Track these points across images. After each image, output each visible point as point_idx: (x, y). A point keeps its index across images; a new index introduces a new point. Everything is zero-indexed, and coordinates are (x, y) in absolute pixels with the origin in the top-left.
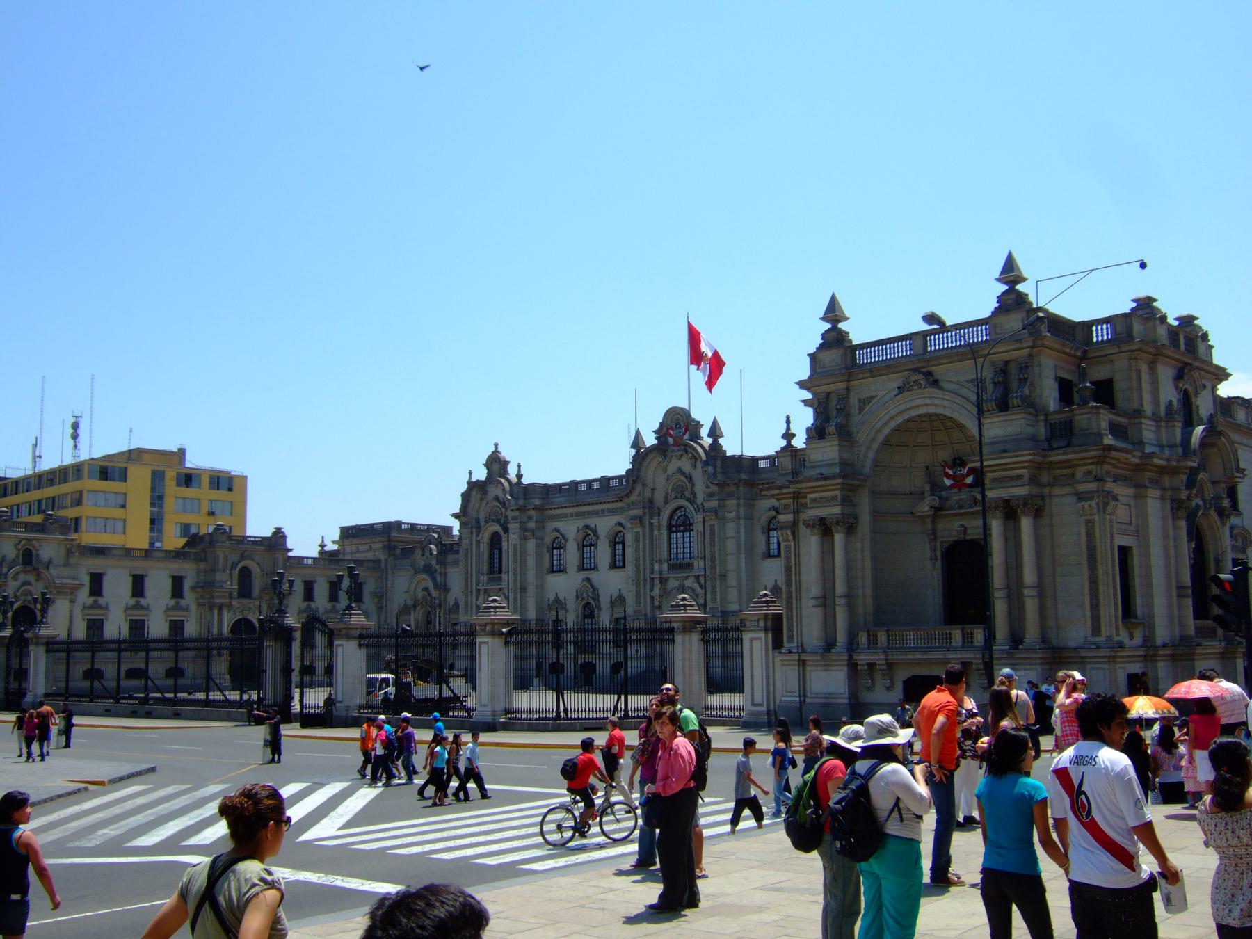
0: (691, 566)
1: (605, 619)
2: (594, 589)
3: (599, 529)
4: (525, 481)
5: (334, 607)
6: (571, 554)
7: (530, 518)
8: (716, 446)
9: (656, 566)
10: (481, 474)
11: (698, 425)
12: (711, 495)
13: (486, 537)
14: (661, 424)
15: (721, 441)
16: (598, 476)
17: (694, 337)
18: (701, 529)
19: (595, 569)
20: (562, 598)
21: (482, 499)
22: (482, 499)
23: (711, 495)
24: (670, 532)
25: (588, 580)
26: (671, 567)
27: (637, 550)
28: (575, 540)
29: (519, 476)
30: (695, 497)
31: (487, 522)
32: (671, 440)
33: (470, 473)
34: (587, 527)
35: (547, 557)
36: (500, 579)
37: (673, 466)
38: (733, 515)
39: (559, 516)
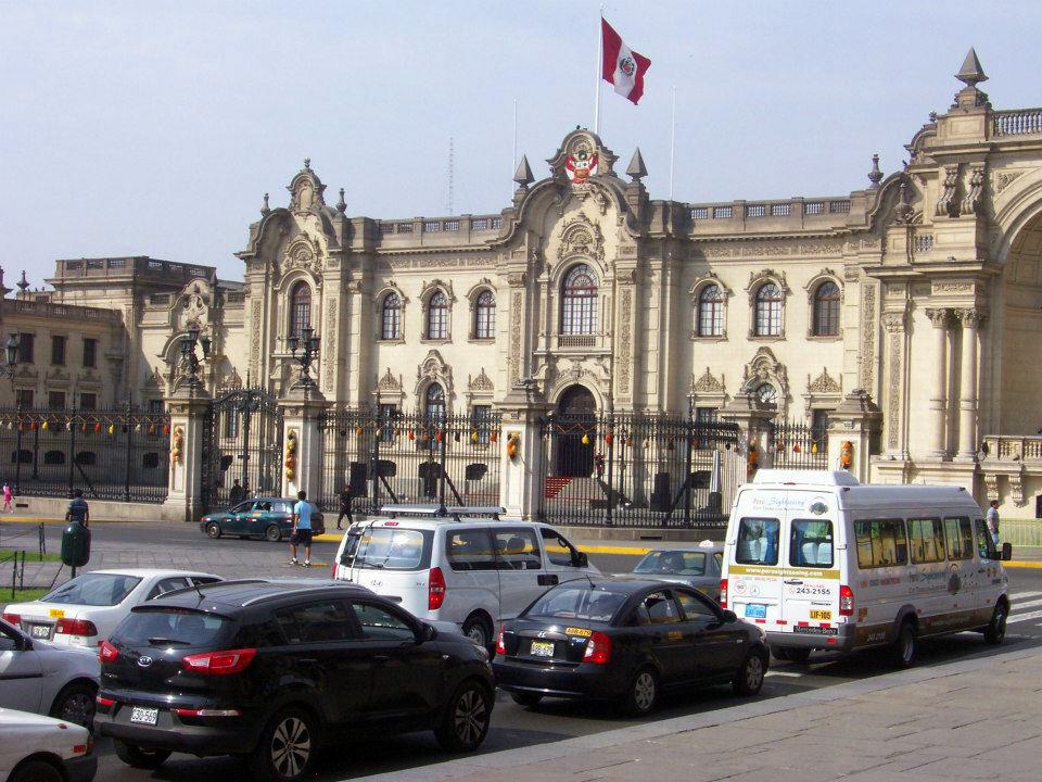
0: (591, 341)
1: (460, 407)
2: (445, 369)
4: (349, 213)
5: (58, 371)
6: (412, 318)
7: (354, 266)
9: (542, 342)
10: (281, 200)
11: (612, 159)
12: (627, 251)
14: (559, 151)
15: (644, 180)
17: (611, 41)
18: (610, 294)
19: (449, 340)
20: (396, 376)
21: (282, 236)
24: (563, 296)
27: (517, 311)
29: (343, 207)
30: (602, 252)
32: (571, 175)
33: (266, 198)
34: (439, 282)
35: (377, 318)
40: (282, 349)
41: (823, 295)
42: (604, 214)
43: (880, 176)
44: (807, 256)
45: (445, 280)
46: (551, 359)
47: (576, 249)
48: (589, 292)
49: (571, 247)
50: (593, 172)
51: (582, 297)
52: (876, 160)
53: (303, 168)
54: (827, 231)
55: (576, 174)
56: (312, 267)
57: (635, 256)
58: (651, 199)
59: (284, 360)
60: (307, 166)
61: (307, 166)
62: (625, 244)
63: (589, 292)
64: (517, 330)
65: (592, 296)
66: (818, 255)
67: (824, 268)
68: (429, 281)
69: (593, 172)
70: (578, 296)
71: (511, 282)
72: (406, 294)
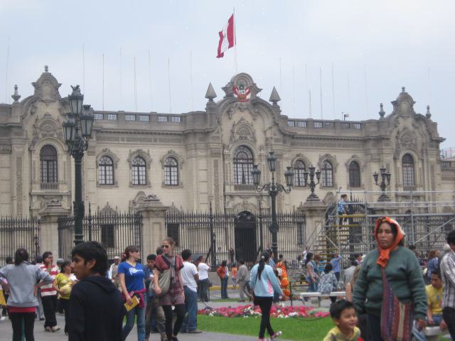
3: (151, 153)
8: (278, 109)
9: (227, 187)
12: (277, 140)
13: (38, 149)
15: (279, 103)
16: (148, 111)
22: (32, 113)
23: (277, 140)
25: (143, 193)
26: (237, 187)
27: (216, 172)
28: (129, 161)
30: (255, 141)
31: (35, 134)
32: (236, 96)
36: (56, 187)
37: (237, 116)
39: (109, 139)
40: (37, 190)
45: (145, 150)
46: (232, 196)
47: (241, 138)
49: (237, 137)
50: (248, 97)
51: (242, 164)
53: (44, 72)
55: (239, 97)
56: (56, 136)
57: (281, 143)
59: (40, 196)
60: (47, 71)
61: (47, 71)
62: (276, 137)
64: (216, 180)
68: (134, 150)
69: (248, 97)
70: (240, 163)
71: (212, 153)
72: (119, 157)
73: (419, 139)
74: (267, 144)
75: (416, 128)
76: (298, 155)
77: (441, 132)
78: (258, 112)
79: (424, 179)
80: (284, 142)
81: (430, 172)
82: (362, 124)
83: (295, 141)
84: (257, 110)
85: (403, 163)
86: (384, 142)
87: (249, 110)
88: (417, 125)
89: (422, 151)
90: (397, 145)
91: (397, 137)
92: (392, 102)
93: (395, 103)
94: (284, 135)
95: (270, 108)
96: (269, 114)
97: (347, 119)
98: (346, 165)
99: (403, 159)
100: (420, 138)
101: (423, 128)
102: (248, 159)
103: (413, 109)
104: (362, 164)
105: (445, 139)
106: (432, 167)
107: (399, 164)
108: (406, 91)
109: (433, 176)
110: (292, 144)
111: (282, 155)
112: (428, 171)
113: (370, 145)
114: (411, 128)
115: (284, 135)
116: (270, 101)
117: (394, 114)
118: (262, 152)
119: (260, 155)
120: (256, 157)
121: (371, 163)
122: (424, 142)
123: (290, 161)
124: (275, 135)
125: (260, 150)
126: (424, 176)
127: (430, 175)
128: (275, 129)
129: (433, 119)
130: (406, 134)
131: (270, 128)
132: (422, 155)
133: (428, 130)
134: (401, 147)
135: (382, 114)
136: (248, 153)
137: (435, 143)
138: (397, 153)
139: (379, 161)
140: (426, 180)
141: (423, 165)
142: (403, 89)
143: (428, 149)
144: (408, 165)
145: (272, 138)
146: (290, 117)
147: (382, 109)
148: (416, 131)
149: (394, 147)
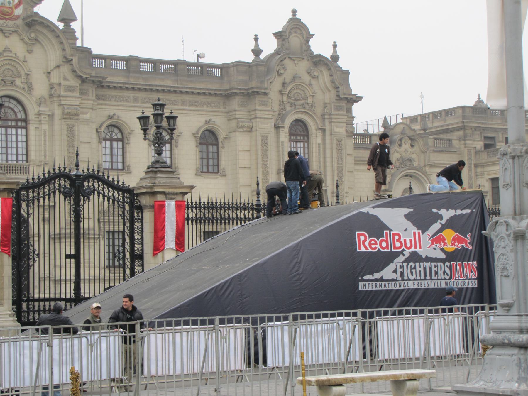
8: (70, 33)
12: (70, 89)
18: (45, 127)
30: (30, 88)
38: (88, 116)
41: (209, 139)
42: (30, 51)
43: (261, 51)
44: (191, 108)
48: (14, 124)
50: (19, 11)
52: (256, 39)
54: (215, 90)
57: (78, 94)
58: (78, 43)
63: (14, 124)
65: (16, 127)
66: (202, 109)
67: (208, 119)
69: (19, 11)
73: (319, 96)
74: (51, 96)
75: (313, 78)
76: (110, 117)
77: (356, 86)
78: (36, 40)
79: (325, 162)
80: (83, 92)
81: (335, 151)
82: (224, 68)
83: (102, 92)
84: (33, 35)
85: (290, 135)
86: (259, 99)
87: (20, 35)
88: (316, 74)
89: (323, 115)
90: (282, 104)
91: (281, 92)
92: (275, 34)
93: (278, 35)
94: (84, 81)
95: (63, 34)
96: (54, 41)
97: (201, 61)
98: (195, 135)
99: (290, 129)
100: (321, 92)
101: (325, 77)
102: (17, 121)
103: (309, 46)
104: (221, 136)
105: (361, 98)
106: (339, 142)
107: (284, 136)
108: (298, 16)
109: (340, 157)
110: (99, 98)
111: (77, 115)
112: (332, 148)
113: (235, 103)
114: (307, 78)
115: (84, 81)
116: (61, 20)
117: (277, 53)
118: (42, 109)
119: (39, 114)
120: (32, 116)
121: (237, 133)
122: (327, 101)
123: (94, 126)
124: (65, 79)
125: (40, 105)
126: (325, 158)
127: (335, 155)
128: (65, 69)
129: (342, 64)
130: (296, 87)
131: (58, 67)
132: (324, 125)
133: (333, 82)
134: (288, 108)
135: (257, 52)
136: (18, 109)
137: (344, 104)
138: (282, 117)
139: (251, 129)
140: (328, 164)
141: (324, 140)
142: (294, 12)
143: (334, 112)
144: (299, 138)
145: (60, 84)
146: (95, 52)
147: (257, 45)
148: (314, 82)
149: (276, 108)
